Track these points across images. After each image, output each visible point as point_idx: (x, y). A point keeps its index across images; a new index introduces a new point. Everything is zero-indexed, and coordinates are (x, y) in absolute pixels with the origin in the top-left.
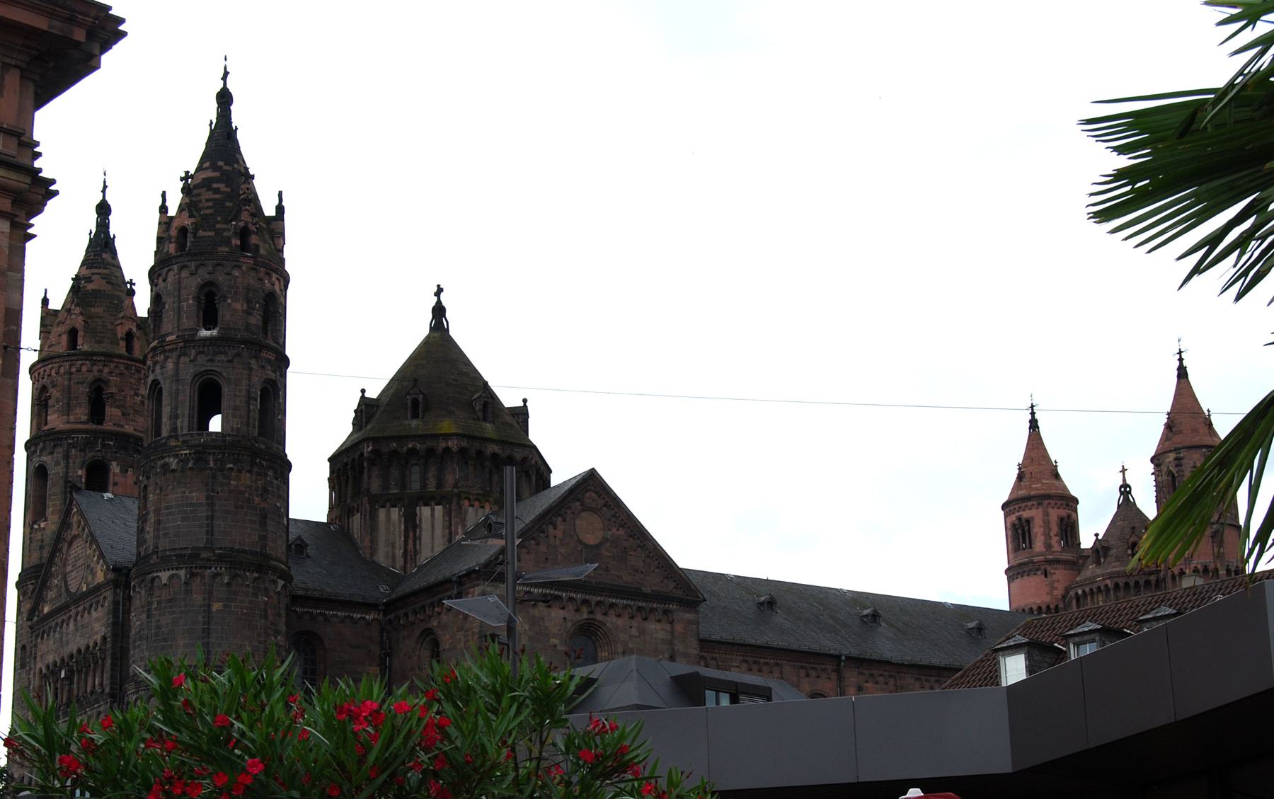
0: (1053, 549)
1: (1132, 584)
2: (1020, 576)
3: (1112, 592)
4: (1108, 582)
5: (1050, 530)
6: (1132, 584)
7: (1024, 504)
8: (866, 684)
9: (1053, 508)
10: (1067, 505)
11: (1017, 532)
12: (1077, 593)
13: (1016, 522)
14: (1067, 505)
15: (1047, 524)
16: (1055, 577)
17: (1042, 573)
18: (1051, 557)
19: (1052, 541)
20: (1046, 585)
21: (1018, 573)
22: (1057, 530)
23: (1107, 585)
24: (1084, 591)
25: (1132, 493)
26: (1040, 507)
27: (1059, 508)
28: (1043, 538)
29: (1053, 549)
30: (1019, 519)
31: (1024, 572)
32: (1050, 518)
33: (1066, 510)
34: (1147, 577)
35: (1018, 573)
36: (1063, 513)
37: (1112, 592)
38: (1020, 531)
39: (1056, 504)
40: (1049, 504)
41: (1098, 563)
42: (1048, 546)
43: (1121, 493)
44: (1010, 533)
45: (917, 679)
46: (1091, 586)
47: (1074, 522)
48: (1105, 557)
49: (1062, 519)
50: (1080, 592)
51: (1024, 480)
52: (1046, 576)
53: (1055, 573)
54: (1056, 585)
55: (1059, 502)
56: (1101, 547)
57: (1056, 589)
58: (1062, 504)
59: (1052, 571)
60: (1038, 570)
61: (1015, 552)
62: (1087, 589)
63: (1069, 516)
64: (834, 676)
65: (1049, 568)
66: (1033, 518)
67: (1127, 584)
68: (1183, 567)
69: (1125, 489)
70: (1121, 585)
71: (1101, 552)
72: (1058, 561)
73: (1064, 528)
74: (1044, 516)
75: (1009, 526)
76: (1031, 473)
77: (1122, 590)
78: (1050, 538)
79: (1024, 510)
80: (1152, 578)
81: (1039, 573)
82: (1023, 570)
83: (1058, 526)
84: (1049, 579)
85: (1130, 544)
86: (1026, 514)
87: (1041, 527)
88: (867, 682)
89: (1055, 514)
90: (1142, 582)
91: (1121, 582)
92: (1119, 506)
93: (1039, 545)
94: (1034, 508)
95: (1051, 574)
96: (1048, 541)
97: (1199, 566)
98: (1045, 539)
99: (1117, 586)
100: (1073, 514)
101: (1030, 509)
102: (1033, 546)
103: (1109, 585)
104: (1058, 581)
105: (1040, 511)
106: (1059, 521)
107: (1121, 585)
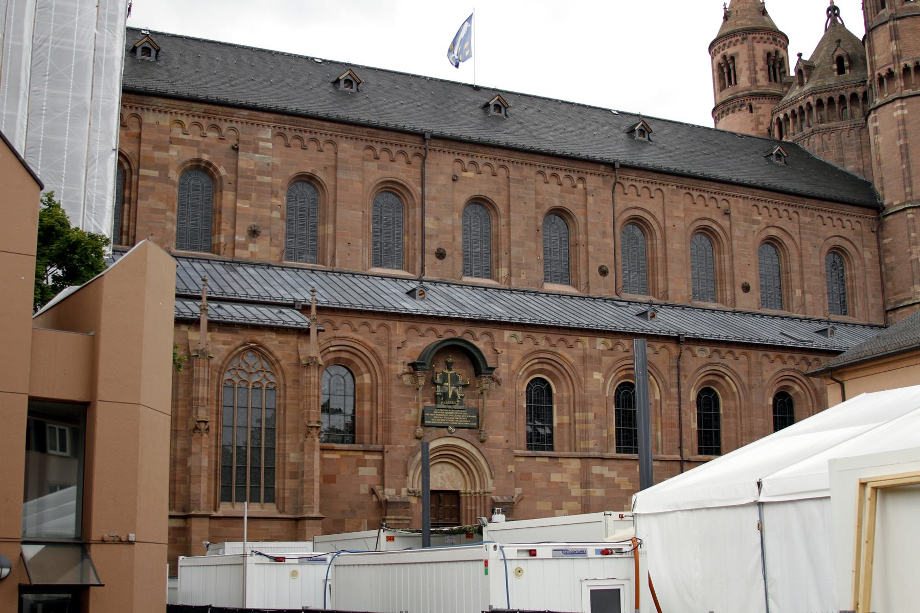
0: (758, 84)
1: (836, 99)
2: (725, 115)
3: (814, 110)
4: (810, 99)
5: (755, 64)
6: (836, 99)
7: (728, 41)
8: (464, 174)
9: (758, 42)
10: (775, 40)
11: (722, 70)
12: (778, 118)
13: (721, 61)
14: (775, 40)
15: (752, 58)
16: (760, 112)
17: (747, 109)
18: (756, 91)
19: (757, 75)
20: (752, 121)
21: (723, 112)
22: (763, 64)
23: (809, 103)
24: (786, 115)
25: (841, 15)
26: (745, 41)
27: (765, 42)
28: (747, 73)
29: (758, 84)
30: (724, 57)
31: (728, 109)
32: (756, 53)
33: (773, 45)
34: (853, 90)
35: (723, 112)
36: (771, 48)
37: (814, 110)
38: (725, 70)
39: (762, 38)
40: (754, 38)
41: (801, 84)
42: (754, 81)
43: (829, 16)
44: (716, 74)
45: (540, 172)
46: (793, 107)
47: (783, 59)
48: (809, 77)
49: (769, 55)
50: (782, 116)
51: (729, 19)
52: (752, 112)
53: (760, 108)
54: (761, 119)
55: (765, 37)
56: (805, 69)
57: (762, 124)
58: (768, 39)
59: (758, 106)
60: (742, 105)
61: (721, 91)
62: (789, 112)
63: (777, 52)
64: (417, 161)
65: (754, 103)
66: (737, 54)
67: (831, 100)
68: (891, 66)
69: (833, 12)
70: (825, 101)
71: (804, 73)
72: (763, 95)
73: (772, 63)
74: (749, 50)
75: (715, 67)
76: (737, 11)
77: (825, 107)
78: (756, 73)
79: (728, 47)
80: (858, 90)
81: (744, 108)
82: (727, 107)
83: (764, 60)
84: (754, 114)
85: (835, 59)
86: (730, 51)
87: (745, 62)
88: (465, 171)
89: (761, 49)
90: (848, 96)
91: (825, 97)
92: (826, 30)
93: (743, 81)
94: (738, 43)
95: (756, 108)
96: (754, 76)
97: (910, 64)
98: (751, 74)
99: (820, 103)
100: (782, 52)
101: (735, 45)
102: (738, 82)
103: (812, 103)
104: (764, 116)
105: (746, 44)
106: (766, 56)
107: (825, 101)
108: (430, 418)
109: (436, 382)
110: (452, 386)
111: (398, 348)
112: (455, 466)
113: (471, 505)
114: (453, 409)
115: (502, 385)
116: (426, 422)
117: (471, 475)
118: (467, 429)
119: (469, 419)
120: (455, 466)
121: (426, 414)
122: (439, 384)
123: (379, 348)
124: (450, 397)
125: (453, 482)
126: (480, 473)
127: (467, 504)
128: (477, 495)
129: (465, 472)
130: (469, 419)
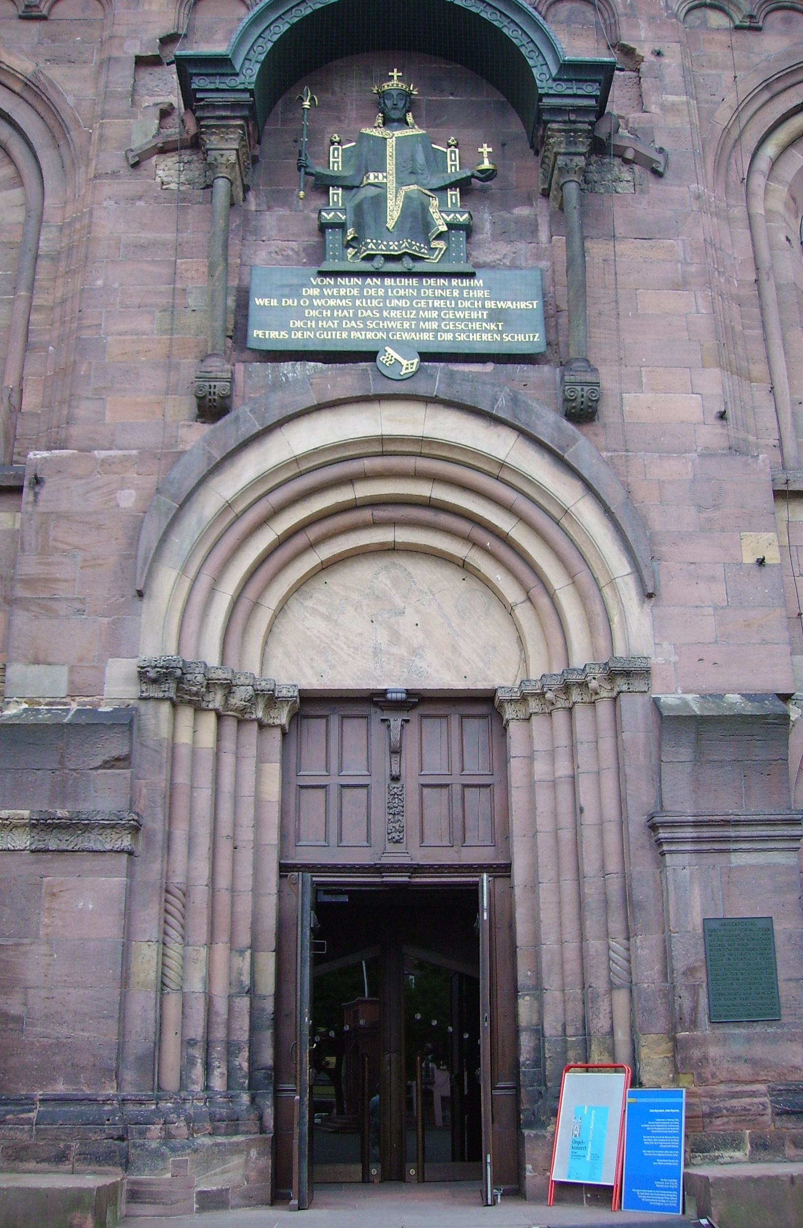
108: (282, 319)
109: (319, 169)
110: (400, 183)
111: (141, 62)
112: (463, 566)
113: (552, 754)
114: (409, 274)
115: (668, 175)
116: (257, 333)
117: (543, 601)
118: (489, 367)
119: (495, 315)
120: (463, 566)
121: (259, 302)
122: (335, 181)
123: (55, 73)
124: (390, 224)
125: (455, 649)
126: (583, 577)
127: (530, 758)
128: (575, 696)
129: (512, 593)
130: (495, 315)
